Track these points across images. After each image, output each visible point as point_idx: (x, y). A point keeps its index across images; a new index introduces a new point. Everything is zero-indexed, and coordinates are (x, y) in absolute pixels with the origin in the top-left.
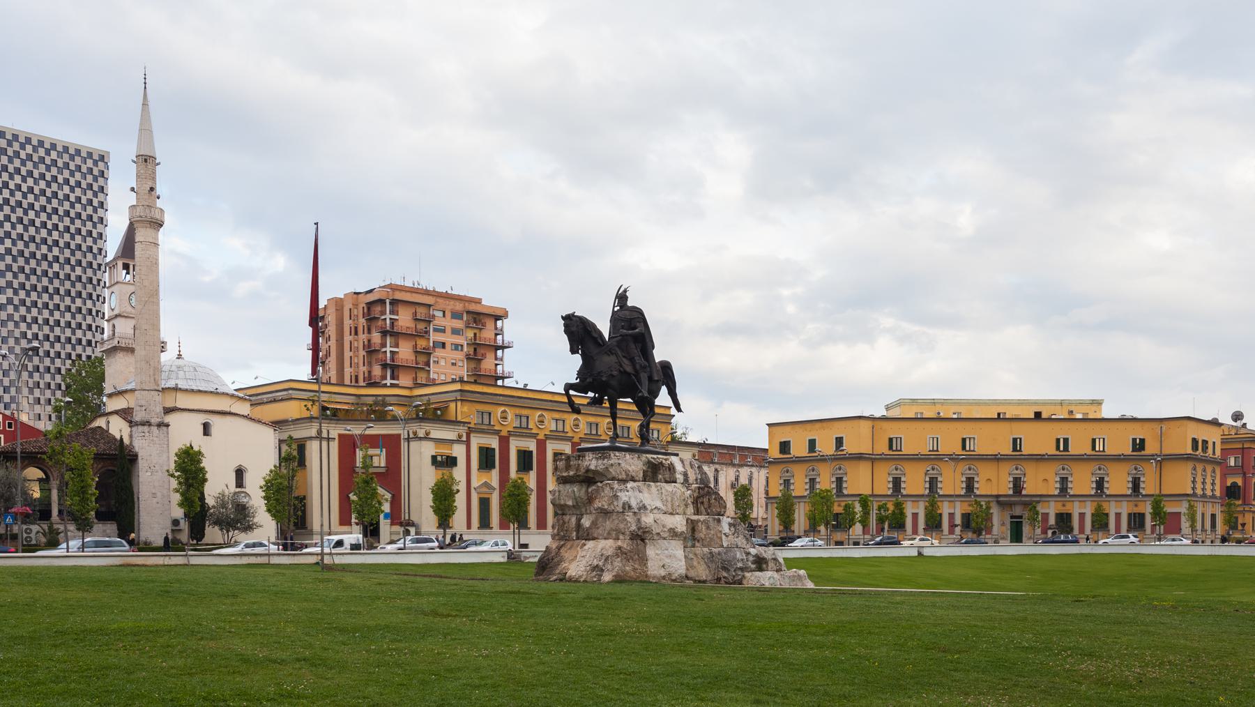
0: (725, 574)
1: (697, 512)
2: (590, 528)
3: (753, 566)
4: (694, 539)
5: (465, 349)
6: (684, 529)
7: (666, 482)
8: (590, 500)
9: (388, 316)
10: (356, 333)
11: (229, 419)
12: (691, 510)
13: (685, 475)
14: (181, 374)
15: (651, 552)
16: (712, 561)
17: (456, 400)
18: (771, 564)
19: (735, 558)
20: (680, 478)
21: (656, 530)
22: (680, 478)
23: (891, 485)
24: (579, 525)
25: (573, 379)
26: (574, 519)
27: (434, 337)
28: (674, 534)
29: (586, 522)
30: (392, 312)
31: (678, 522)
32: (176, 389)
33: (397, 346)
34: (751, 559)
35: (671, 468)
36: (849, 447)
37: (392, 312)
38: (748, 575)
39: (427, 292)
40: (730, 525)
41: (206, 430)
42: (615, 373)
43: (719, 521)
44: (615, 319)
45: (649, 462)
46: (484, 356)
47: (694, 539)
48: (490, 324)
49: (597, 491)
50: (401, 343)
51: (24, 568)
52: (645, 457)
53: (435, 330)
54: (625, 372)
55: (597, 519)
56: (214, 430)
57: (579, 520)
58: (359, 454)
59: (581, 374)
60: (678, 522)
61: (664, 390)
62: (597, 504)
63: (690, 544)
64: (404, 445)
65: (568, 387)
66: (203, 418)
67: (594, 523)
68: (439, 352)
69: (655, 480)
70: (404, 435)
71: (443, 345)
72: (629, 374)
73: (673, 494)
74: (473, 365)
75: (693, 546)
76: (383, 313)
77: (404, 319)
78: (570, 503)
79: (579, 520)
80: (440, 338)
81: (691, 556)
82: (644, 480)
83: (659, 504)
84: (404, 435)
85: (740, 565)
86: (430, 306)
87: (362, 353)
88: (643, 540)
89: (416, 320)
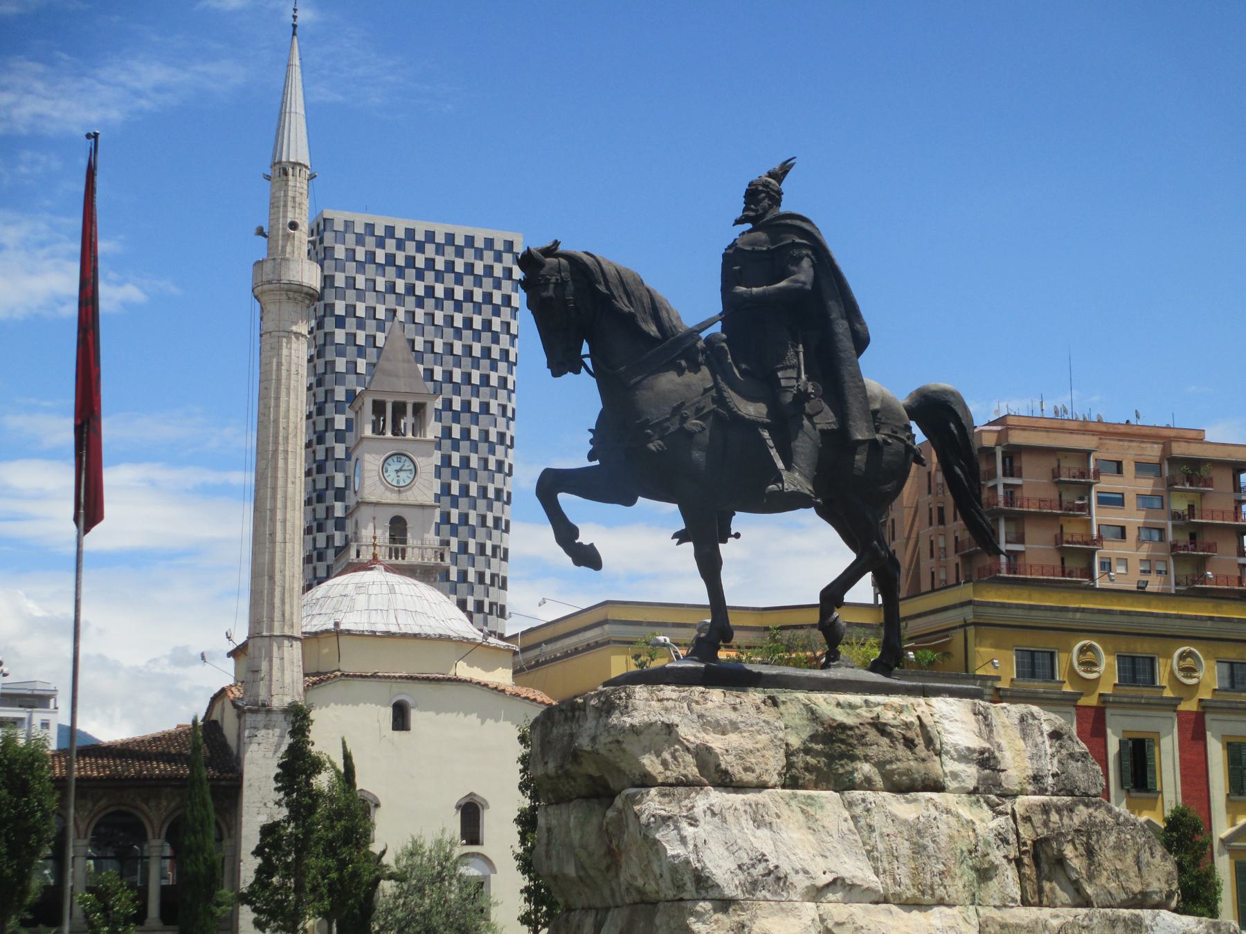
5: (1170, 536)
9: (1001, 481)
10: (942, 521)
11: (449, 688)
13: (987, 760)
14: (361, 600)
17: (965, 625)
25: (575, 454)
27: (1099, 516)
30: (1009, 472)
32: (337, 633)
33: (1020, 540)
35: (924, 738)
36: (1149, 588)
37: (1009, 472)
39: (1084, 428)
41: (401, 718)
42: (693, 423)
44: (737, 264)
46: (1211, 547)
48: (1223, 480)
49: (621, 823)
50: (1030, 531)
53: (1103, 501)
56: (415, 716)
59: (605, 436)
65: (550, 486)
68: (1110, 549)
69: (843, 784)
71: (1122, 533)
73: (918, 833)
74: (1187, 571)
76: (992, 475)
77: (1034, 484)
80: (1113, 516)
82: (791, 781)
83: (858, 870)
86: (1088, 453)
87: (954, 559)
89: (1059, 483)
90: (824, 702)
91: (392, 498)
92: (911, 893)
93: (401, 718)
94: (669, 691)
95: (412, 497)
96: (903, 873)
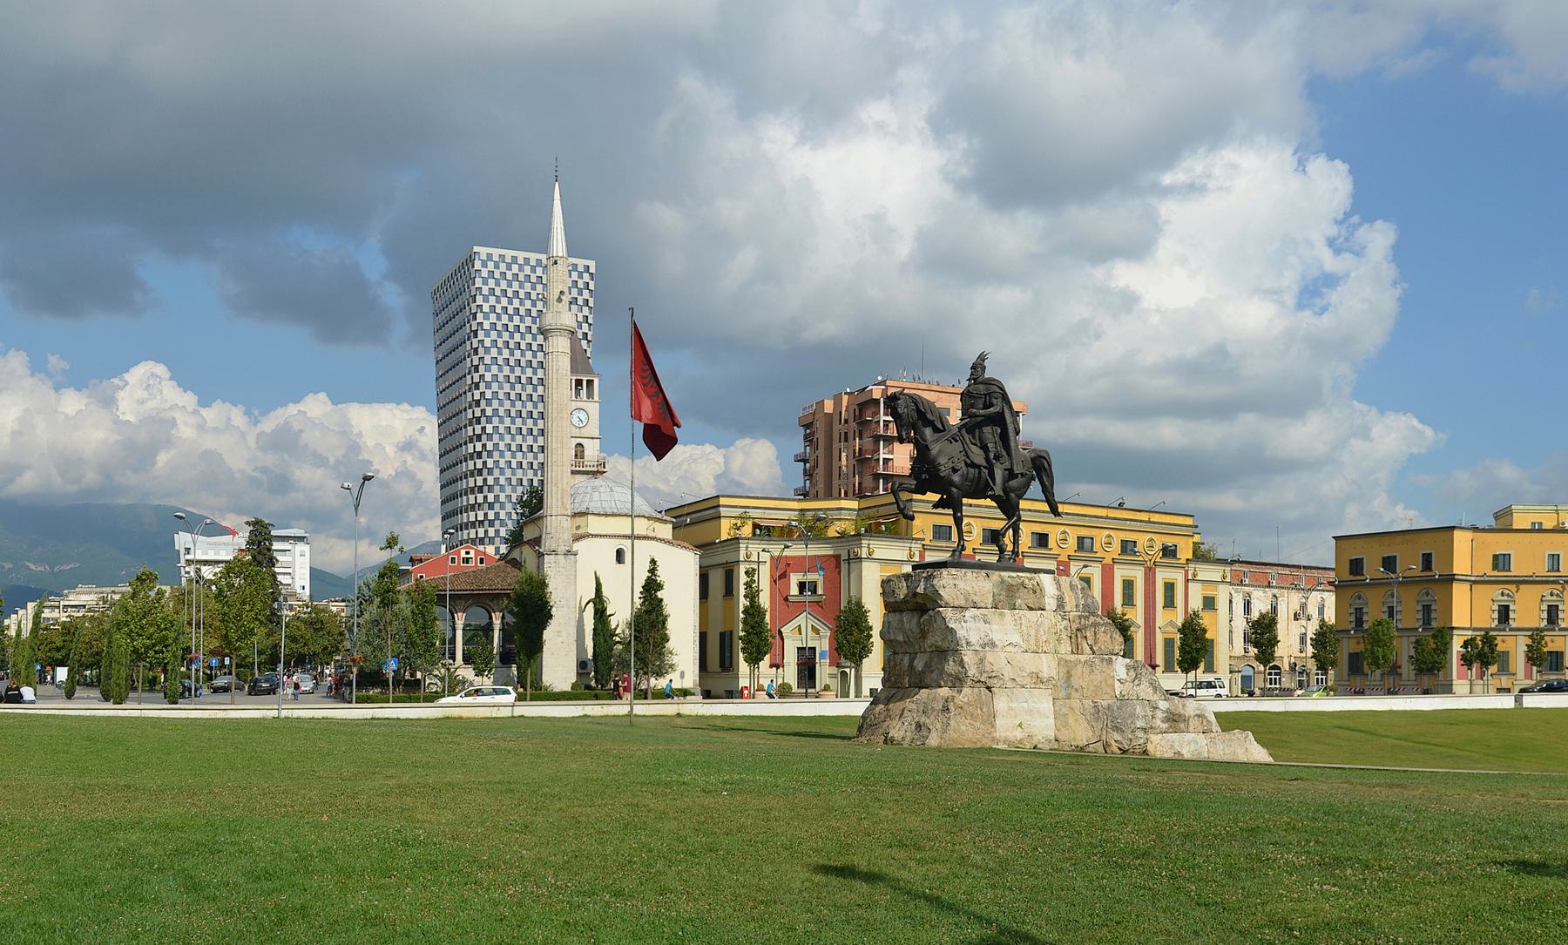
0: (1117, 737)
1: (1077, 650)
2: (923, 672)
3: (1164, 726)
4: (1069, 686)
6: (1054, 673)
7: (1031, 609)
8: (923, 634)
12: (1066, 647)
15: (1001, 703)
16: (1097, 719)
18: (1193, 723)
19: (1133, 715)
20: (1050, 603)
21: (1008, 672)
22: (1050, 603)
23: (1496, 615)
24: (911, 666)
26: (906, 659)
28: (1038, 680)
29: (919, 664)
31: (1047, 666)
34: (1160, 715)
35: (1037, 590)
38: (1153, 737)
40: (1128, 667)
43: (1110, 661)
45: (1003, 581)
47: (1069, 686)
49: (930, 622)
51: (94, 717)
52: (995, 575)
54: (973, 465)
55: (931, 659)
57: (912, 661)
58: (795, 579)
60: (1047, 666)
61: (1035, 487)
62: (930, 640)
63: (1063, 694)
64: (844, 566)
66: (616, 544)
67: (927, 665)
70: (844, 556)
72: (978, 467)
75: (1068, 697)
78: (900, 638)
79: (912, 661)
81: (1064, 710)
83: (1016, 639)
84: (844, 556)
85: (1139, 724)
88: (989, 688)
90: (1005, 574)
91: (576, 432)
92: (1034, 648)
93: (620, 555)
94: (953, 571)
95: (586, 432)
96: (1033, 641)
